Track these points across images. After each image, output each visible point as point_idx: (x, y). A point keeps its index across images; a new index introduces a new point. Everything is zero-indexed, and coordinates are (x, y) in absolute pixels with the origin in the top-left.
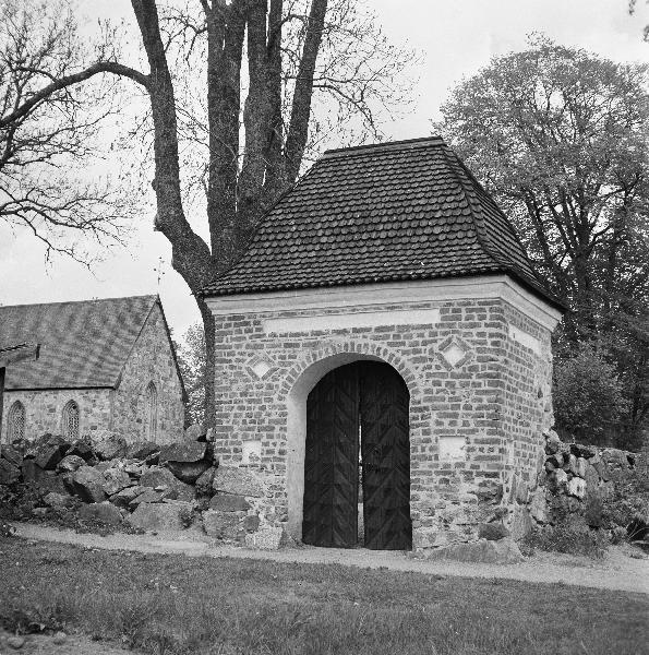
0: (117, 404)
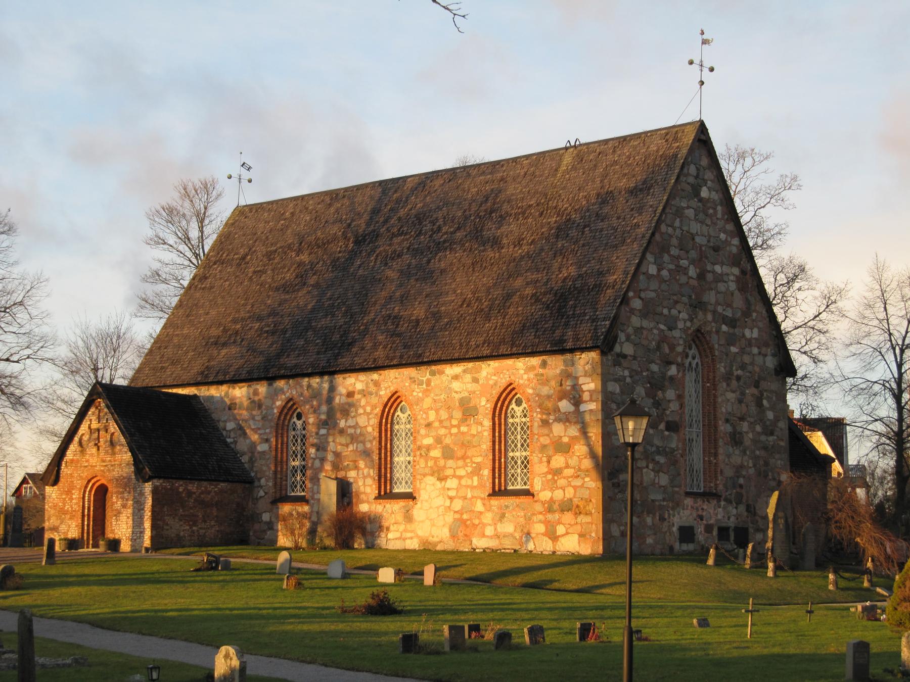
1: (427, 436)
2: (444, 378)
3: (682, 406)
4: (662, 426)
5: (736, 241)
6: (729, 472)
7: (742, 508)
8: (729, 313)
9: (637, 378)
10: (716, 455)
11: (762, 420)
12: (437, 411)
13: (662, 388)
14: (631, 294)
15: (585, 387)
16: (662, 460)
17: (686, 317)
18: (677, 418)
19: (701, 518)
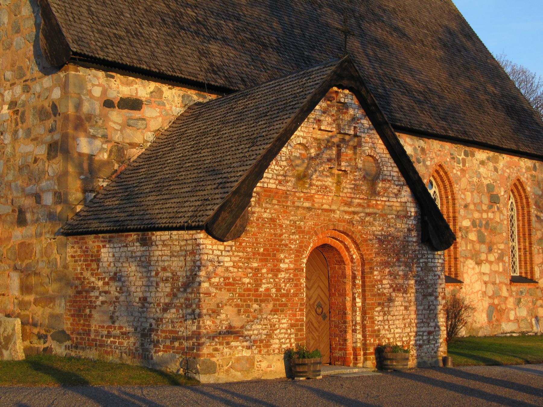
1: (465, 218)
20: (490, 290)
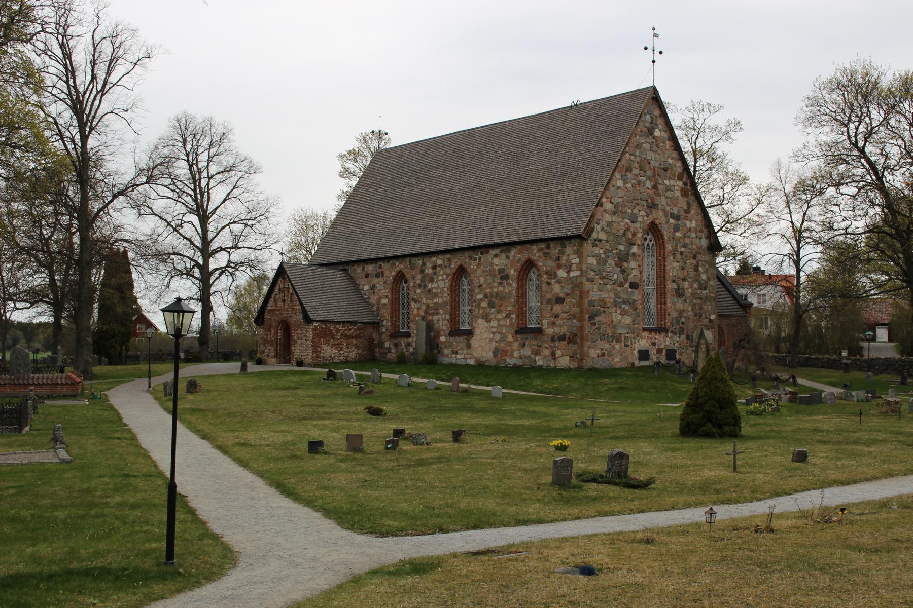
0: (592, 261)
1: (480, 293)
2: (489, 256)
3: (641, 272)
4: (627, 285)
5: (679, 164)
6: (675, 314)
7: (683, 337)
8: (675, 211)
9: (609, 254)
10: (665, 304)
11: (697, 279)
12: (485, 277)
13: (627, 261)
14: (604, 200)
15: (573, 261)
16: (627, 307)
17: (644, 214)
18: (637, 281)
19: (654, 344)
20: (498, 337)
